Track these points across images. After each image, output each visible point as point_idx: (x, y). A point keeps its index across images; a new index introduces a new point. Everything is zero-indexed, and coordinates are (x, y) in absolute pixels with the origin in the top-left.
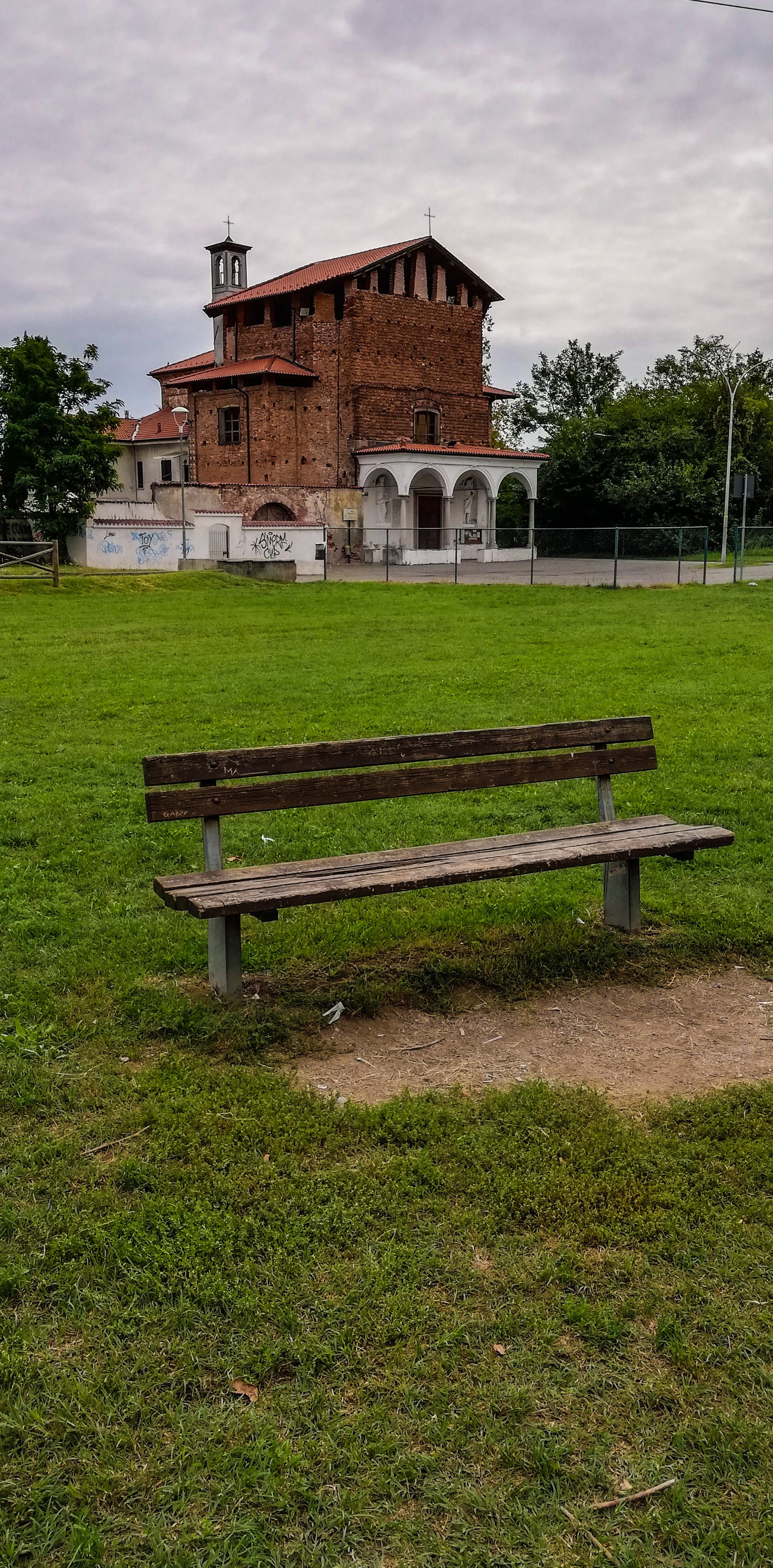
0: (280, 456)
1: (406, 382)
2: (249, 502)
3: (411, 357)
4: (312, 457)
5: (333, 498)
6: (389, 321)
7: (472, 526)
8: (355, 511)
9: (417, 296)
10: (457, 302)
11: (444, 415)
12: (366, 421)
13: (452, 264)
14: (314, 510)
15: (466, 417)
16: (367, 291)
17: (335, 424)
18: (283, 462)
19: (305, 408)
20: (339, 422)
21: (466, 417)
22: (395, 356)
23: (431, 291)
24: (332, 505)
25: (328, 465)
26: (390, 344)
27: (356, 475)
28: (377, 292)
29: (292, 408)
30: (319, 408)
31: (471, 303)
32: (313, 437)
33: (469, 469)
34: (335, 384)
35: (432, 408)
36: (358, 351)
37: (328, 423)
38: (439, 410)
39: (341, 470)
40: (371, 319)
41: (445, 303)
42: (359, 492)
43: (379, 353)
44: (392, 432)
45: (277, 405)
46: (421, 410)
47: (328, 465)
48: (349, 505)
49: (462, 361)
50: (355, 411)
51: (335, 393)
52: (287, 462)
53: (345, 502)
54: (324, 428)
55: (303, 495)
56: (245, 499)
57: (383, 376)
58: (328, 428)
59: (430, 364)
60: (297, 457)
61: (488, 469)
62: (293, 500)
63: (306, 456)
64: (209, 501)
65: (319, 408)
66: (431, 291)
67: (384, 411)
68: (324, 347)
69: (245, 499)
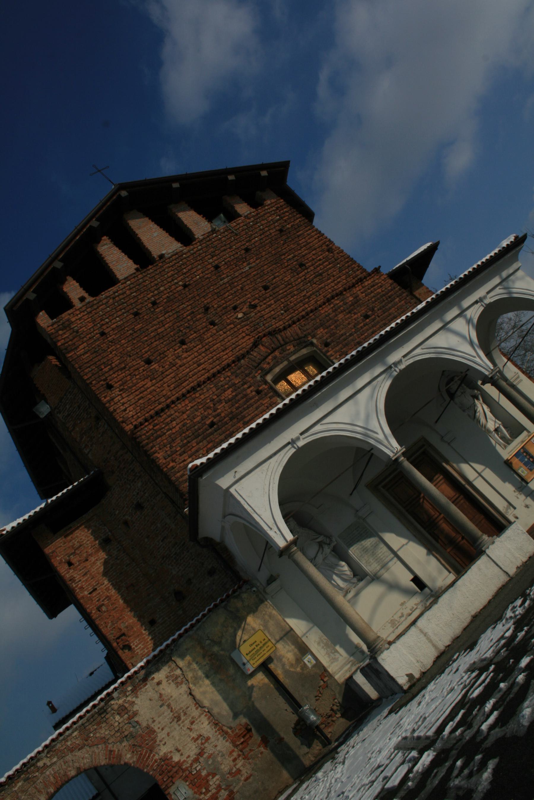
1: (227, 357)
6: (136, 314)
9: (162, 256)
10: (232, 216)
14: (168, 714)
19: (126, 523)
22: (183, 343)
23: (183, 235)
25: (211, 573)
28: (89, 299)
30: (139, 506)
31: (255, 204)
36: (110, 387)
38: (312, 344)
40: (103, 334)
43: (148, 362)
45: (74, 560)
49: (301, 265)
59: (254, 307)
62: (104, 740)
65: (139, 506)
66: (183, 235)
67: (212, 424)
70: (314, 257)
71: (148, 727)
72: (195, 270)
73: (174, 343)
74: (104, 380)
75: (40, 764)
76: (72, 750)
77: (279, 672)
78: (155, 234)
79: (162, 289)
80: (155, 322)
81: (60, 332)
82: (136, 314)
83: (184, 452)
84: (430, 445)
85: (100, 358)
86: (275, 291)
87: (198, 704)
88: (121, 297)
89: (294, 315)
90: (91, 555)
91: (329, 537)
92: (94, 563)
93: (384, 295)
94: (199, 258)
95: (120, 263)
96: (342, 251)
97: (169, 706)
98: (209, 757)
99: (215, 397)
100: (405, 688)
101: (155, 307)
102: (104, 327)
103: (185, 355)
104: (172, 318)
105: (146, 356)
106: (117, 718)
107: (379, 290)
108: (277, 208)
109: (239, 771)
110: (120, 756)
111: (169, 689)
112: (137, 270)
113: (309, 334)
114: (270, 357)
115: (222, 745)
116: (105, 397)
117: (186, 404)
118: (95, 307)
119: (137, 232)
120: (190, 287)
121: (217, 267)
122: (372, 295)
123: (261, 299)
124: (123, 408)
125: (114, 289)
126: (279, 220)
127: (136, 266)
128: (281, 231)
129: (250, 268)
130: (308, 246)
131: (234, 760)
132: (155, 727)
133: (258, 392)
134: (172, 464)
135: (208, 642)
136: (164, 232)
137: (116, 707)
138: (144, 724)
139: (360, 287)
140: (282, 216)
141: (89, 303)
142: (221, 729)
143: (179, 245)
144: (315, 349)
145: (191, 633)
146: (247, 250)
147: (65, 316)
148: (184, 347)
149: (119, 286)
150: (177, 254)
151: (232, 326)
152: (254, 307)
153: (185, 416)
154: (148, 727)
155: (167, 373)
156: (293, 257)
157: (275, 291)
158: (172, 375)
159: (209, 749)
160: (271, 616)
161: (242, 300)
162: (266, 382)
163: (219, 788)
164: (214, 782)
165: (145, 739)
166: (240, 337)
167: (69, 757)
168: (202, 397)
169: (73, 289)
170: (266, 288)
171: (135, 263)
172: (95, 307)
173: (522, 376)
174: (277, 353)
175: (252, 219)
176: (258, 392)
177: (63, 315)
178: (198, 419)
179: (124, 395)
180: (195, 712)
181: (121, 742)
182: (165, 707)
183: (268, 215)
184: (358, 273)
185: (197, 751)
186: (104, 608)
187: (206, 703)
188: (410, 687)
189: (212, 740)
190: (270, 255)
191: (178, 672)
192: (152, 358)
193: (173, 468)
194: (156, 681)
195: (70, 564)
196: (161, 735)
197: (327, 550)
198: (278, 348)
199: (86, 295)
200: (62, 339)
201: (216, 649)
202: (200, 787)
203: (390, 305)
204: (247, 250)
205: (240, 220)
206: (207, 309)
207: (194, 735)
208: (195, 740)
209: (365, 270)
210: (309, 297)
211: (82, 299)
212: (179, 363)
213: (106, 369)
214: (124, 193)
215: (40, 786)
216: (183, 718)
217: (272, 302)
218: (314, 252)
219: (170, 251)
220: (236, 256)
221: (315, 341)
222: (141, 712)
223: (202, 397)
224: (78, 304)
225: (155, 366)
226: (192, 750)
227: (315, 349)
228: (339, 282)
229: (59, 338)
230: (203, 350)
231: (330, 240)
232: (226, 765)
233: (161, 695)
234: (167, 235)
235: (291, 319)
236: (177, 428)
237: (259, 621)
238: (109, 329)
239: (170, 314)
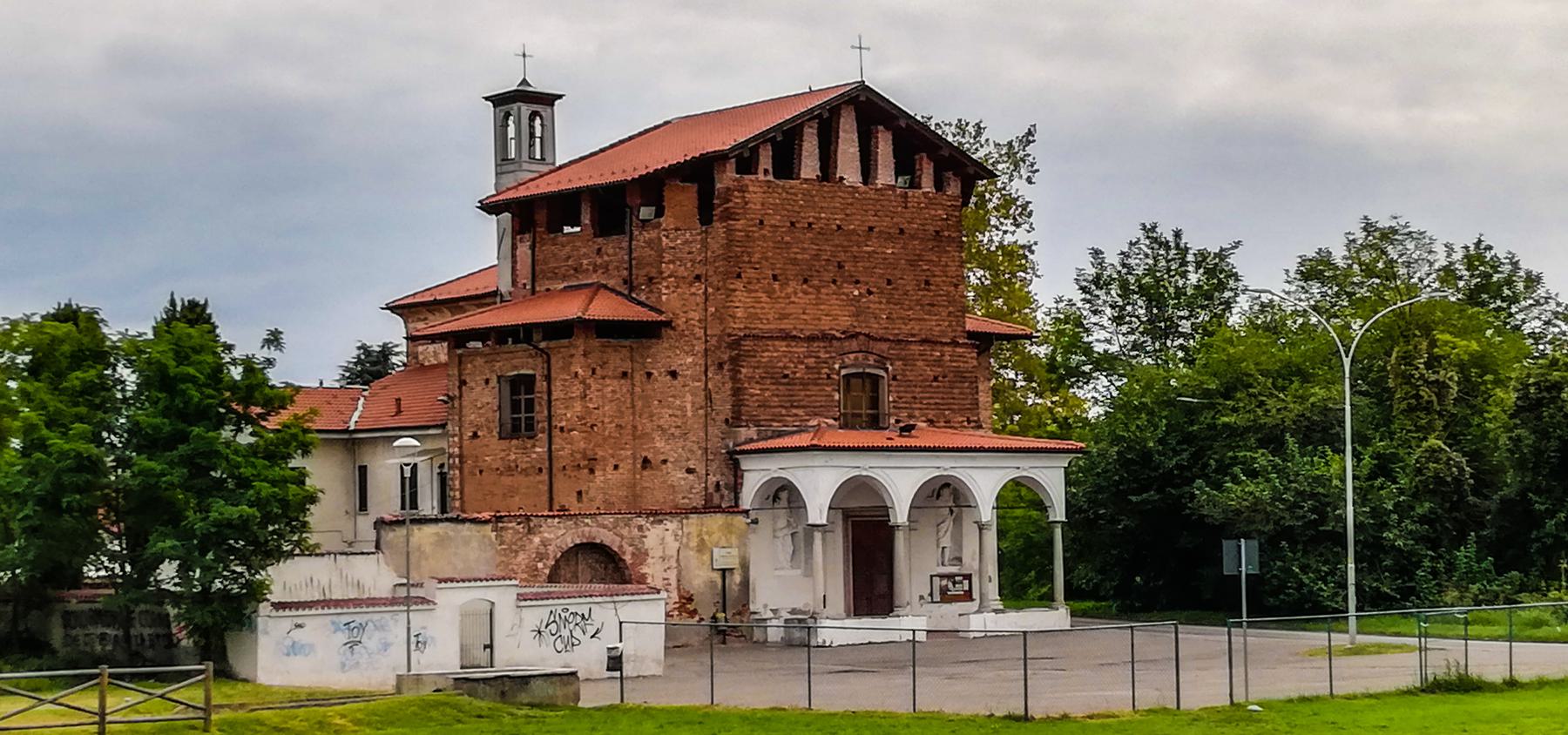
0: (604, 458)
1: (826, 324)
2: (544, 543)
3: (834, 282)
6: (793, 224)
8: (735, 552)
9: (842, 179)
10: (914, 184)
11: (894, 378)
15: (936, 379)
16: (753, 177)
17: (701, 400)
18: (610, 469)
19: (649, 375)
20: (708, 397)
21: (936, 379)
22: (805, 281)
23: (868, 171)
24: (694, 543)
25: (689, 471)
26: (794, 262)
27: (736, 488)
28: (770, 178)
29: (625, 374)
30: (674, 374)
31: (939, 185)
32: (662, 422)
34: (700, 332)
35: (870, 366)
36: (739, 276)
37: (689, 398)
38: (886, 370)
39: (712, 479)
40: (761, 222)
41: (893, 188)
42: (740, 520)
43: (775, 278)
44: (800, 412)
45: (599, 371)
46: (854, 371)
47: (689, 471)
48: (723, 543)
49: (927, 283)
50: (734, 379)
51: (699, 347)
52: (616, 467)
53: (715, 537)
54: (682, 408)
55: (640, 528)
56: (537, 540)
57: (783, 317)
58: (689, 406)
59: (870, 293)
60: (635, 459)
62: (622, 537)
64: (474, 544)
65: (674, 374)
66: (868, 171)
67: (786, 376)
68: (682, 271)
69: (537, 540)
82: (793, 224)
111: (669, 538)
117: (782, 346)
121: (871, 229)
132: (651, 553)
133: (829, 377)
146: (902, 231)
152: (870, 293)
165: (641, 555)
169: (766, 160)
170: (889, 282)
176: (829, 377)
196: (650, 560)
224: (761, 177)
225: (776, 285)
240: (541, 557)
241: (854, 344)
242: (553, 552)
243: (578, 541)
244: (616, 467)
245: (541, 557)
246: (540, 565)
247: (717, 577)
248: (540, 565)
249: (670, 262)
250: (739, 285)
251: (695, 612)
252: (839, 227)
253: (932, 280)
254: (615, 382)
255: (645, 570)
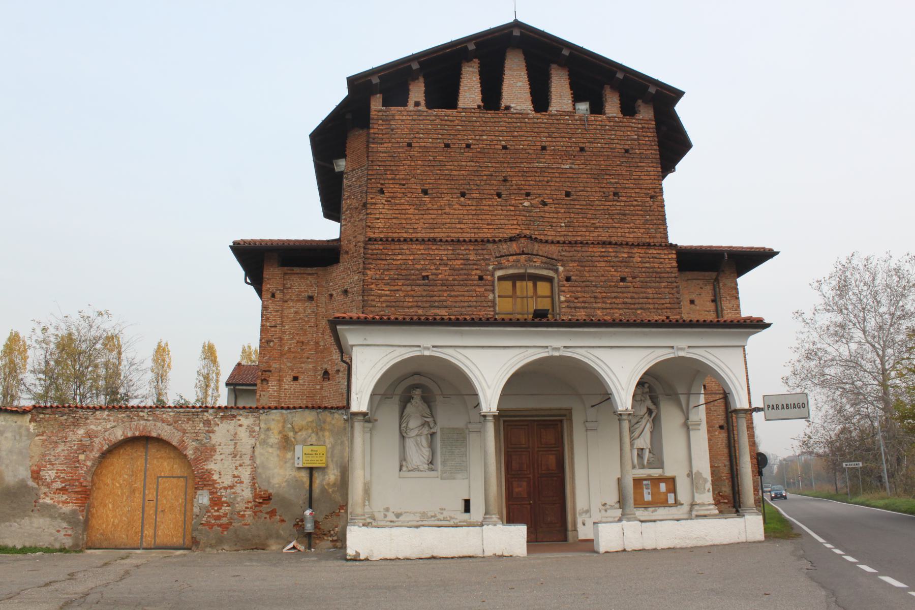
2: (90, 435)
3: (499, 195)
4: (336, 368)
5: (275, 427)
7: (656, 473)
9: (508, 108)
10: (597, 108)
11: (568, 279)
12: (380, 296)
13: (566, 52)
14: (231, 449)
15: (623, 279)
18: (288, 380)
19: (331, 295)
21: (623, 279)
22: (463, 195)
24: (274, 438)
28: (423, 108)
29: (311, 298)
30: (346, 292)
31: (628, 110)
33: (542, 354)
36: (382, 192)
38: (556, 271)
40: (409, 145)
41: (571, 114)
43: (425, 192)
45: (279, 295)
48: (314, 438)
55: (207, 423)
59: (544, 204)
60: (315, 370)
61: (596, 352)
63: (329, 368)
64: (9, 435)
67: (425, 278)
69: (81, 432)
70: (633, 195)
71: (214, 445)
72: (524, 138)
73: (456, 191)
74: (382, 184)
75: (141, 414)
76: (163, 421)
77: (317, 482)
78: (519, 84)
79: (485, 137)
80: (456, 164)
81: (380, 122)
82: (447, 146)
83: (388, 284)
84: (571, 420)
85: (392, 163)
86: (572, 202)
87: (253, 458)
88: (448, 123)
89: (570, 234)
90: (292, 300)
91: (435, 423)
92: (290, 308)
93: (657, 273)
94: (536, 130)
95: (470, 92)
96: (664, 206)
97: (235, 444)
98: (234, 493)
99: (445, 258)
100: (348, 557)
101: (467, 150)
102: (415, 140)
103: (457, 207)
104: (471, 169)
105: (427, 187)
106: (201, 425)
107: (656, 265)
108: (643, 128)
109: (244, 516)
110: (186, 448)
111: (243, 434)
112: (479, 107)
113: (562, 261)
114: (515, 257)
115: (247, 494)
116: (372, 198)
118: (421, 118)
119: (506, 72)
120: (508, 151)
121: (544, 148)
122: (647, 265)
123: (556, 202)
124: (378, 216)
125: (449, 112)
126: (634, 140)
127: (481, 103)
128: (627, 151)
129: (571, 168)
130: (637, 182)
131: (247, 508)
132: (218, 449)
133: (481, 278)
134: (373, 286)
135: (290, 426)
136: (528, 87)
137: (205, 418)
138: (213, 442)
139: (643, 251)
140: (641, 138)
141: (419, 111)
142: (254, 484)
143: (531, 107)
144: (555, 276)
145: (284, 411)
146: (582, 149)
147: (394, 109)
148: (462, 199)
149: (453, 112)
150: (523, 115)
151: (512, 208)
152: (544, 204)
153: (411, 257)
154: (214, 445)
155: (431, 212)
156: (616, 183)
157: (572, 202)
158: (433, 216)
159: (238, 489)
160: (342, 443)
161: (539, 192)
162: (493, 275)
163: (225, 515)
164: (225, 509)
165: (207, 451)
166: (511, 222)
167: (159, 424)
168: (436, 252)
169: (417, 92)
170: (568, 194)
171: (483, 100)
172: (421, 118)
173: (704, 427)
174: (523, 258)
175: (612, 124)
176: (481, 278)
177: (393, 108)
178: (419, 267)
179: (386, 207)
180: (247, 461)
181: (193, 441)
182: (233, 443)
183: (629, 129)
184: (659, 235)
185: (230, 484)
186: (272, 344)
187: (258, 461)
188: (351, 560)
189: (244, 485)
190: (598, 167)
191: (257, 429)
192: (430, 192)
193: (371, 290)
194: (240, 422)
195: (273, 296)
196: (217, 457)
197: (426, 431)
198: (528, 254)
199: (423, 102)
200: (377, 128)
201: (291, 434)
202: (216, 505)
203: (653, 284)
204: (582, 149)
205: (600, 117)
206: (505, 180)
207: (236, 473)
208: (235, 477)
209: (667, 238)
210: (596, 228)
211: (417, 104)
212: (447, 211)
213: (390, 177)
214: (516, 33)
215: (133, 426)
216: (238, 457)
217: (562, 211)
218: (637, 191)
219: (519, 108)
220: (569, 149)
221: (561, 269)
222: (217, 434)
223: (436, 252)
224: (411, 106)
225: (426, 199)
226: (227, 481)
227: (555, 276)
228: (634, 232)
229: (375, 126)
230: (474, 212)
231: (661, 189)
232: (240, 506)
233: (236, 434)
234: (528, 91)
235: (565, 235)
236: (399, 262)
237: (332, 440)
238: (417, 145)
239: (473, 164)
240: (83, 448)
241: (514, 247)
242: (100, 444)
243: (130, 435)
244: (296, 379)
245: (83, 448)
246: (82, 457)
247: (304, 476)
248: (82, 457)
249: (349, 197)
250: (381, 199)
251: (272, 513)
252: (505, 148)
253: (622, 192)
254: (299, 305)
255: (211, 466)
